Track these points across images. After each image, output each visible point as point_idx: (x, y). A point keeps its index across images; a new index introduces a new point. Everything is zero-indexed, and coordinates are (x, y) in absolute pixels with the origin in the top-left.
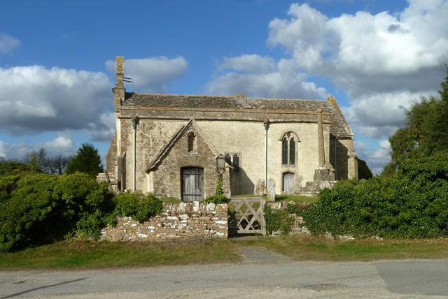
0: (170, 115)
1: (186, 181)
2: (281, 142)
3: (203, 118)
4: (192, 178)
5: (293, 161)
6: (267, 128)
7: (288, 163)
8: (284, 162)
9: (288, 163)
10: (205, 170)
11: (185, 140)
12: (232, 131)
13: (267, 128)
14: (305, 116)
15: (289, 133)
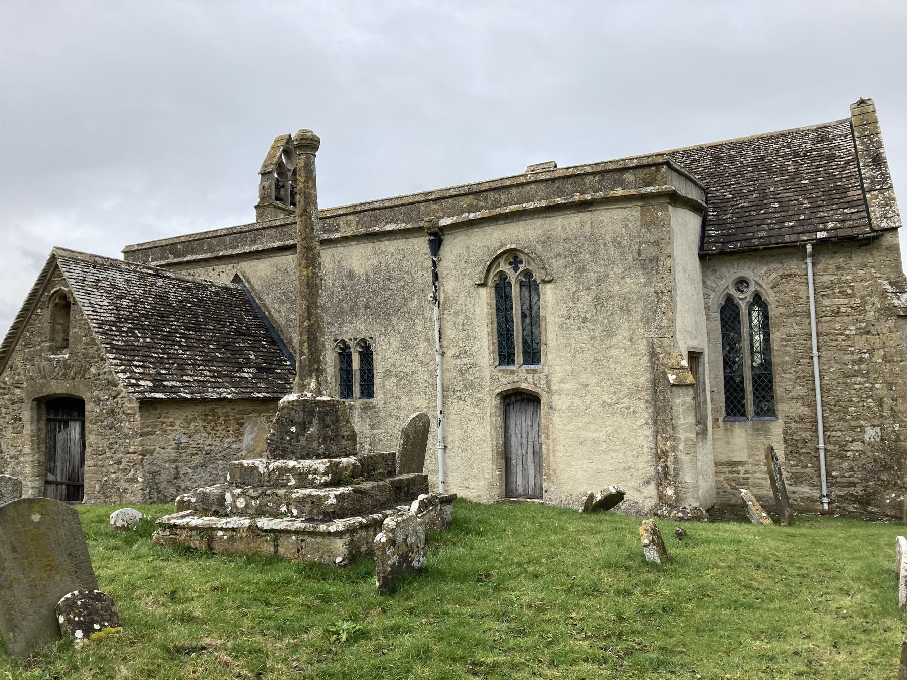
0: (210, 250)
1: (60, 437)
2: (486, 295)
3: (276, 245)
4: (74, 429)
5: (533, 355)
6: (436, 245)
7: (519, 358)
8: (505, 356)
9: (519, 358)
10: (88, 407)
11: (44, 315)
12: (351, 275)
13: (436, 245)
14: (568, 186)
15: (513, 256)
